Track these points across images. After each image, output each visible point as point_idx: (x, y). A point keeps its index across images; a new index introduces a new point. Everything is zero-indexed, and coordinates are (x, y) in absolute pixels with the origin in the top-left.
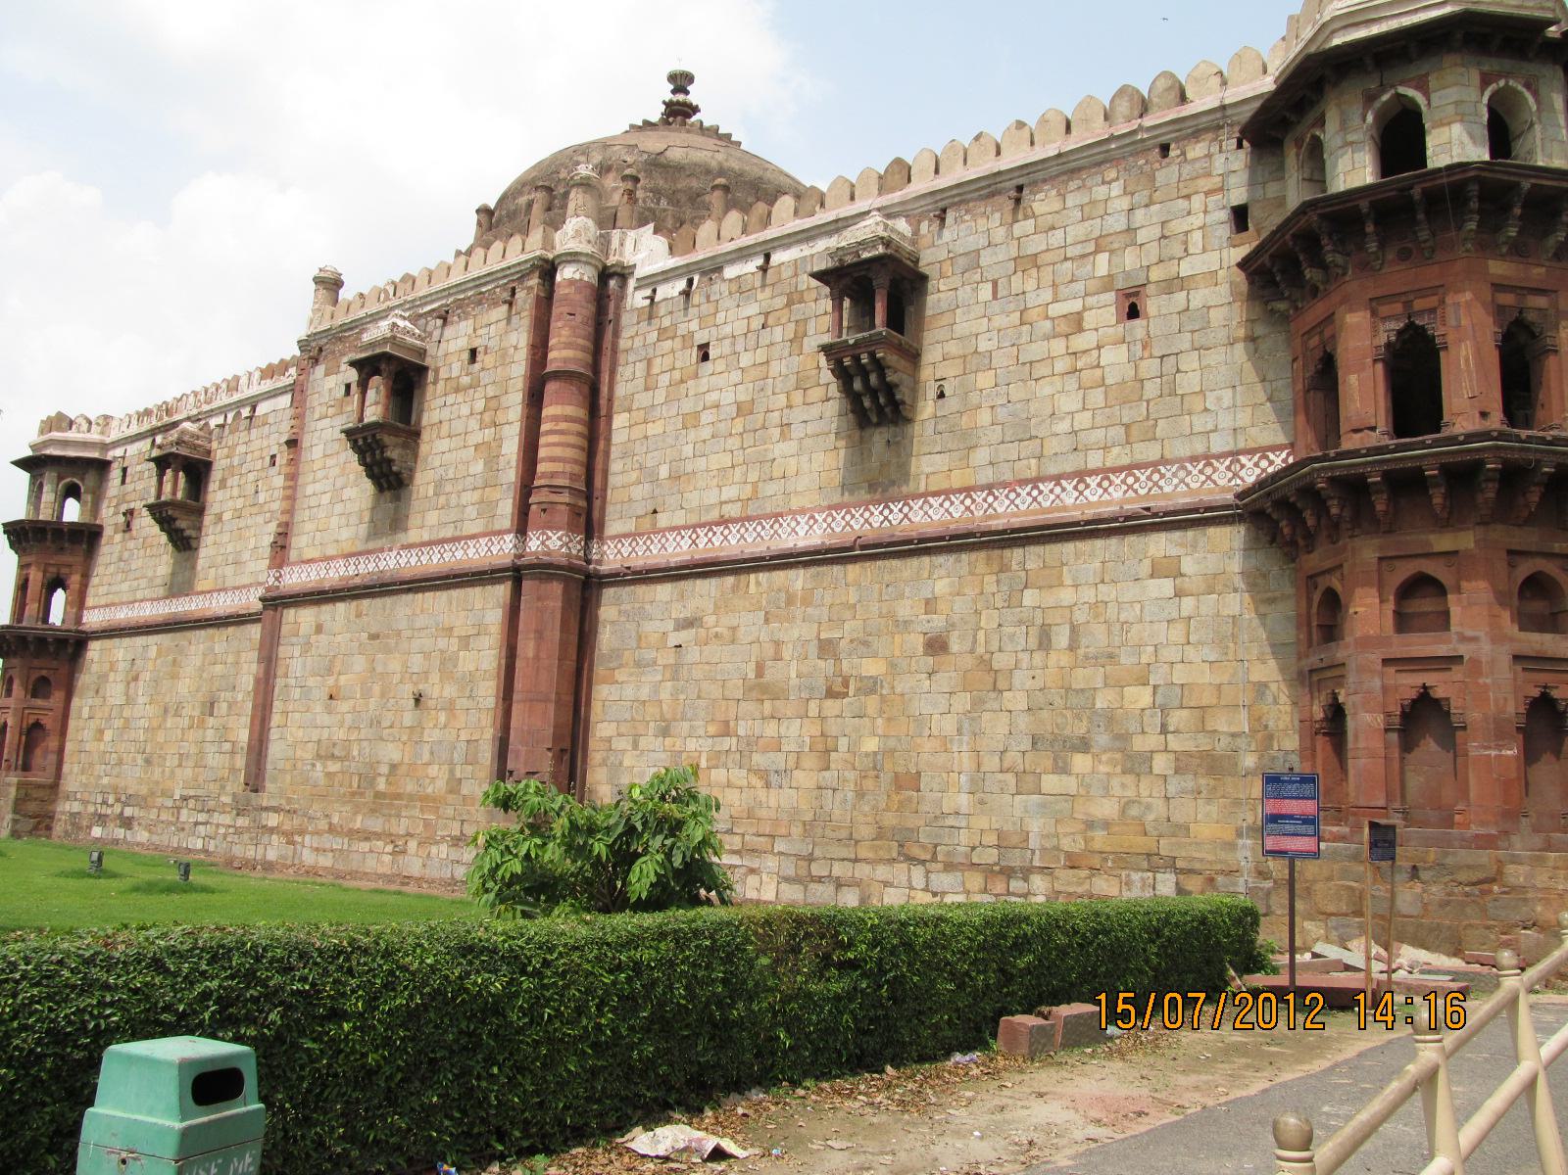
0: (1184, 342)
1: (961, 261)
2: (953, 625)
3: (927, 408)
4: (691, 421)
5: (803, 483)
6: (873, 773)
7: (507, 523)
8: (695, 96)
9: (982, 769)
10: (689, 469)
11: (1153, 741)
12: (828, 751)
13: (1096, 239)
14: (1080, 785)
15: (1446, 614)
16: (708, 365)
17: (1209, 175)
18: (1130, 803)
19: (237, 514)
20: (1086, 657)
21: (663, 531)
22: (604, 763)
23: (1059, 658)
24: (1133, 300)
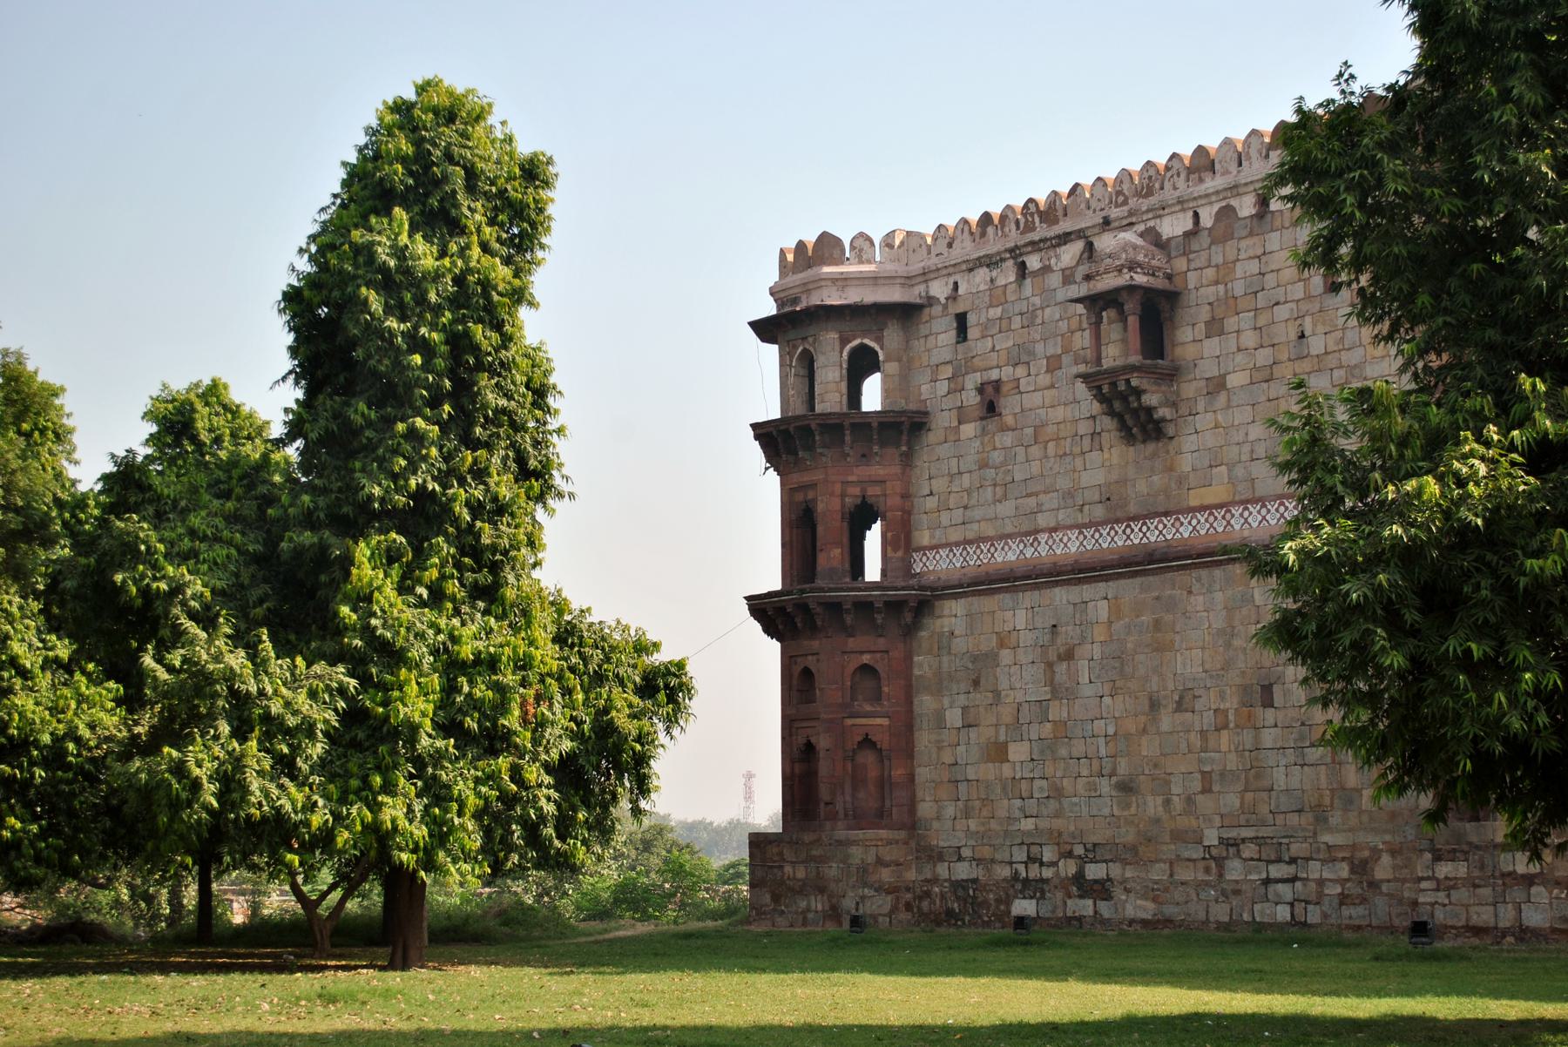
19: (1258, 376)
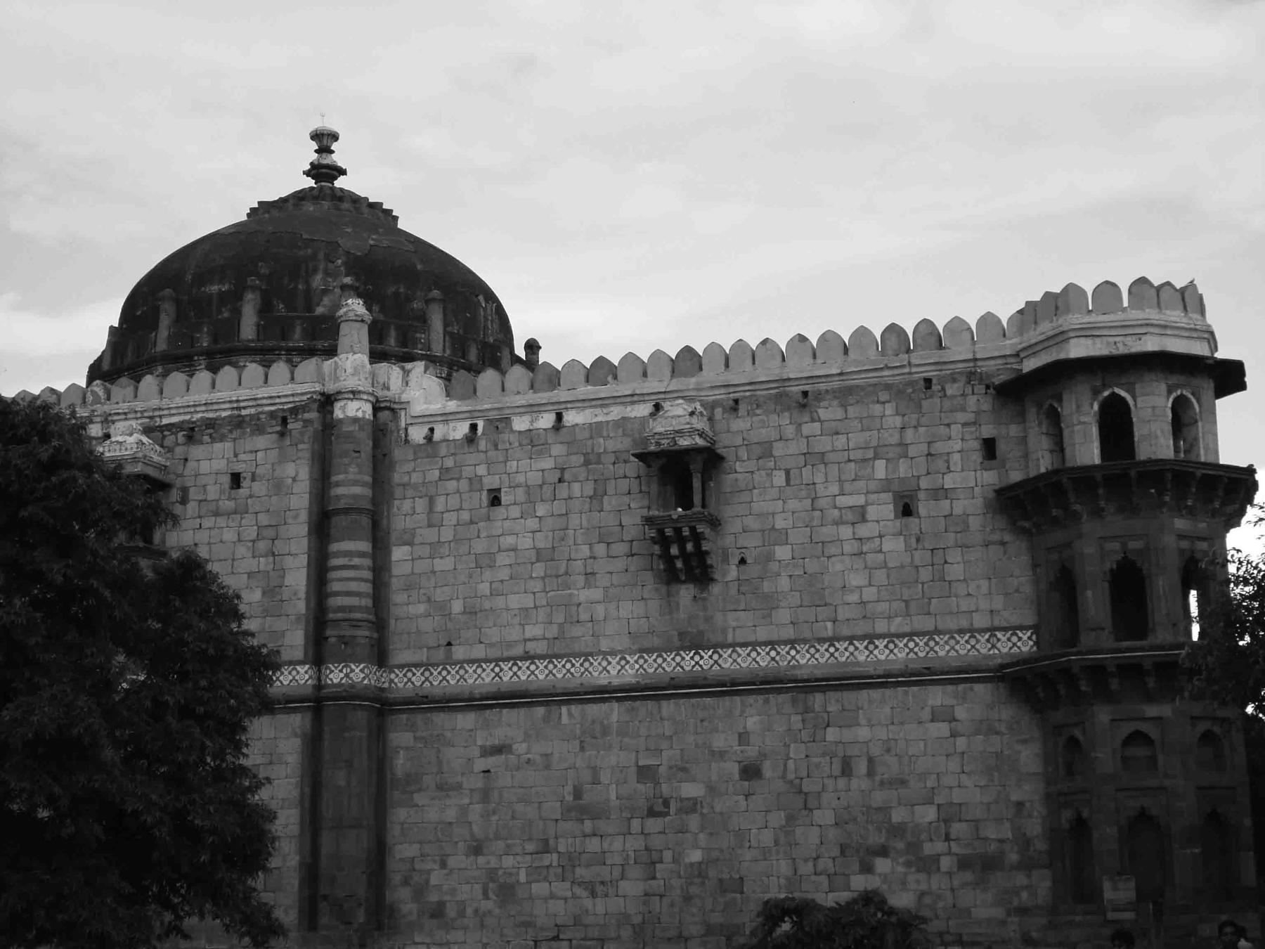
0: (951, 538)
1: (757, 450)
2: (765, 755)
3: (733, 572)
4: (485, 562)
5: (611, 628)
6: (697, 880)
7: (299, 654)
8: (339, 156)
9: (799, 873)
10: (487, 605)
11: (940, 846)
12: (654, 863)
13: (875, 448)
14: (884, 882)
15: (1153, 760)
16: (500, 512)
17: (963, 409)
18: (923, 894)
20: (882, 783)
21: (461, 663)
22: (406, 882)
23: (860, 782)
24: (907, 500)
